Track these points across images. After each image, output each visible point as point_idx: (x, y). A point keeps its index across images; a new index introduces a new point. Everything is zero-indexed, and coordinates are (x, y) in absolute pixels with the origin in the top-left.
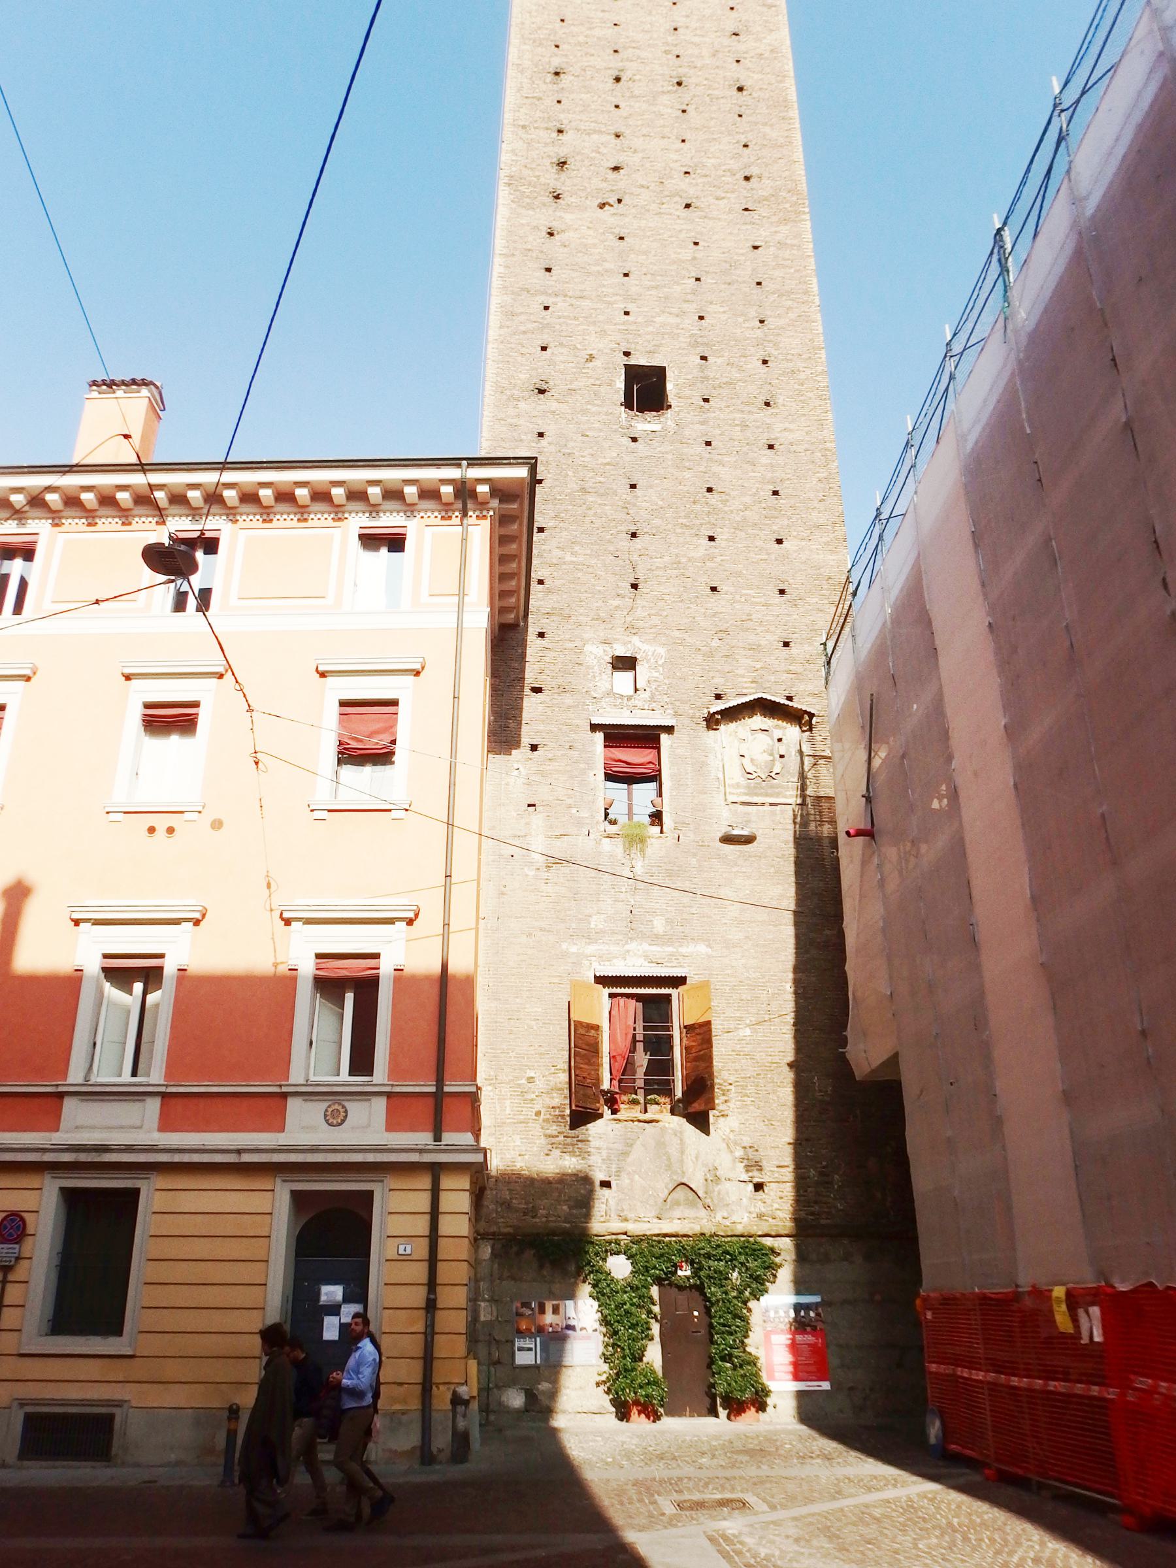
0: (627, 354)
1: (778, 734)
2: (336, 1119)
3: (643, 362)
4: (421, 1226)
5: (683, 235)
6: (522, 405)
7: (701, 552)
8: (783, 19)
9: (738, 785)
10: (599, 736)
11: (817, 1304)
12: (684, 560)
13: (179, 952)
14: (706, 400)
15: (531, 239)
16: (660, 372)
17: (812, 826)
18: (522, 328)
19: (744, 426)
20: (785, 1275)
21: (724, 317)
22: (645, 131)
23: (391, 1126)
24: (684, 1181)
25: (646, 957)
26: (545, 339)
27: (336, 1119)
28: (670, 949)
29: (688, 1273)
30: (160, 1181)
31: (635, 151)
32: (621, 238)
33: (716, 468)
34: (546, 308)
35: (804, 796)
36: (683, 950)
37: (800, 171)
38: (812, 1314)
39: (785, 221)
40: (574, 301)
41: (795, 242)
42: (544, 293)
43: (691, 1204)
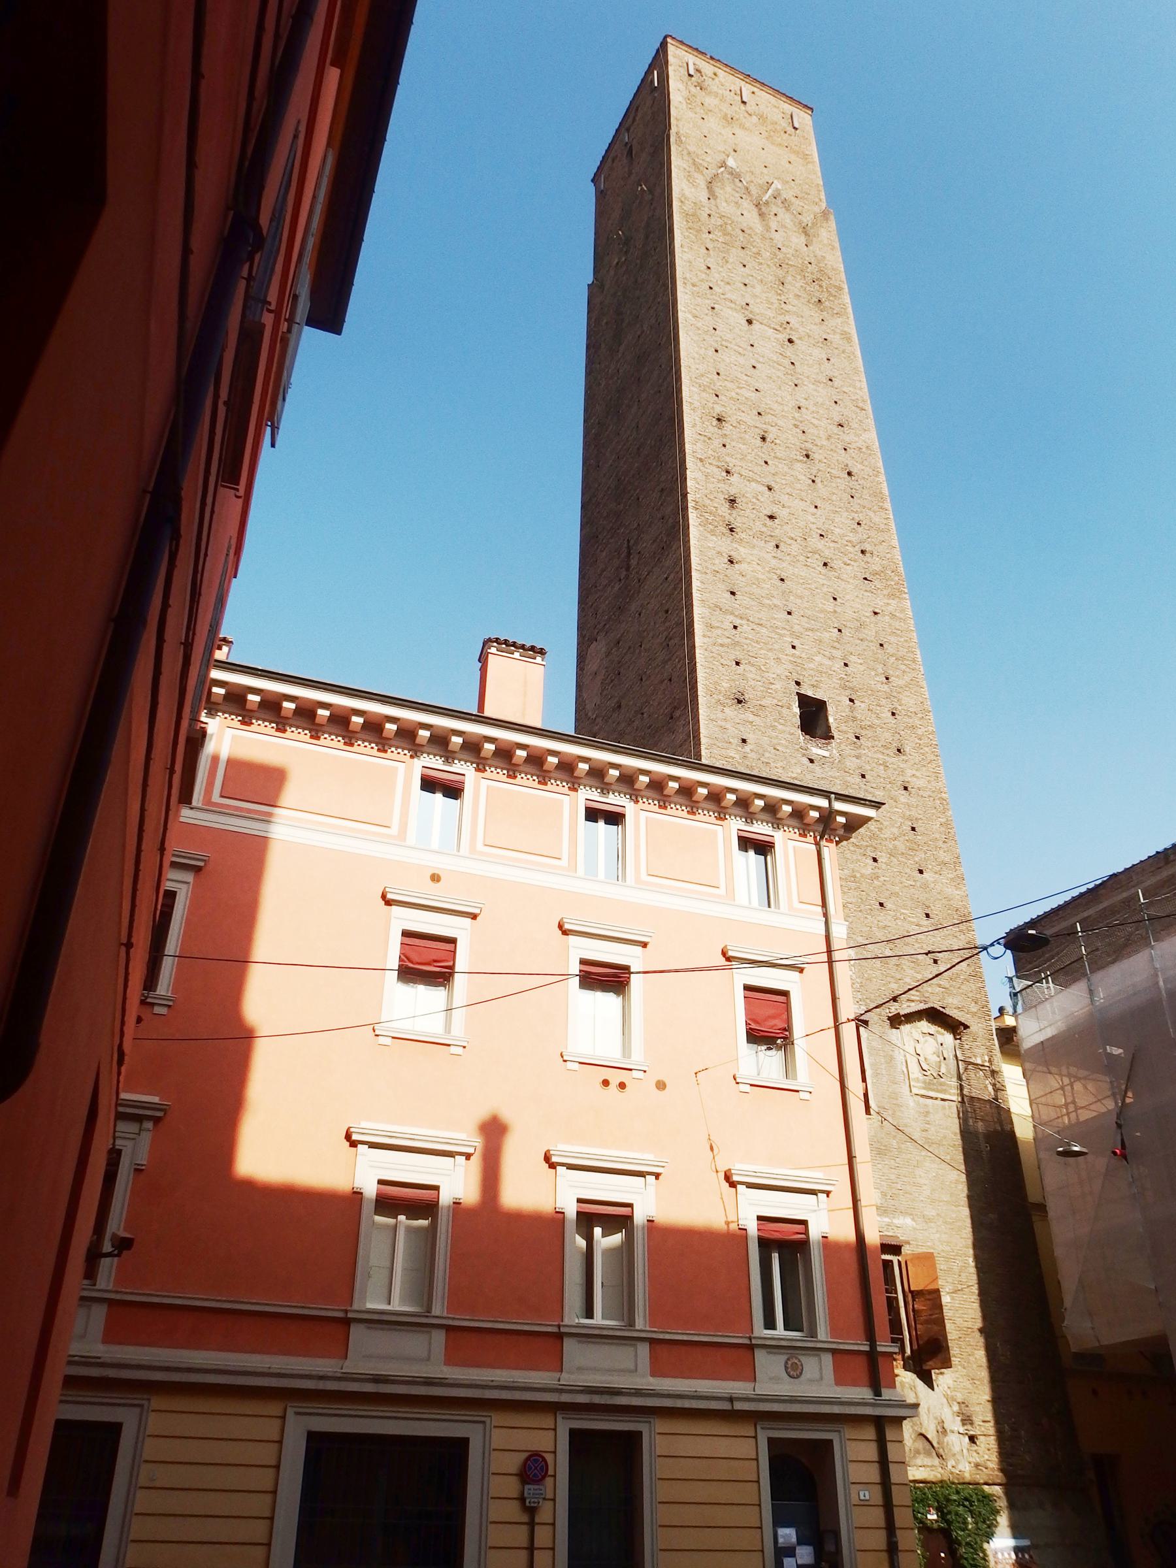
0: (798, 683)
1: (940, 1039)
2: (794, 1371)
3: (810, 693)
4: (873, 1474)
5: (825, 590)
6: (727, 710)
8: (871, 422)
9: (917, 1080)
11: (1028, 1547)
12: (858, 875)
13: (647, 1203)
14: (857, 738)
15: (717, 562)
17: (971, 1122)
18: (720, 641)
20: (1003, 1520)
21: (862, 668)
22: (788, 490)
23: (839, 1381)
24: (923, 1432)
26: (739, 656)
27: (794, 1371)
28: (887, 1220)
29: (935, 1517)
30: (661, 1425)
31: (783, 506)
32: (782, 580)
34: (735, 627)
35: (962, 1095)
36: (896, 1221)
37: (897, 554)
38: (1027, 1556)
40: (755, 627)
41: (902, 616)
42: (732, 614)
43: (928, 1454)
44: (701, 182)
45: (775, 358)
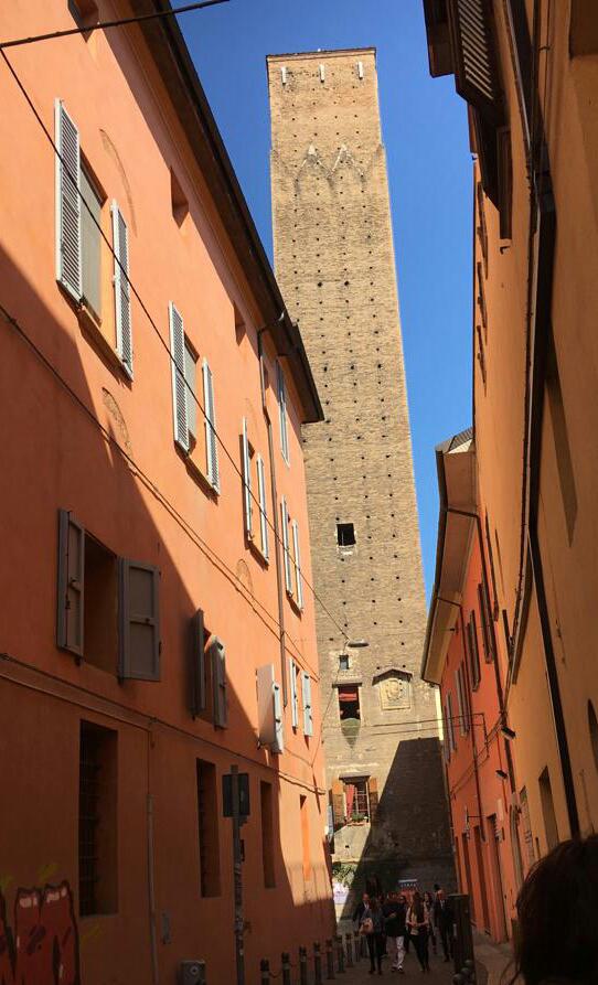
3: (344, 522)
7: (369, 608)
10: (337, 690)
16: (352, 525)
19: (385, 548)
25: (357, 769)
33: (374, 569)
37: (406, 409)
39: (400, 440)
44: (290, 183)
45: (335, 304)
